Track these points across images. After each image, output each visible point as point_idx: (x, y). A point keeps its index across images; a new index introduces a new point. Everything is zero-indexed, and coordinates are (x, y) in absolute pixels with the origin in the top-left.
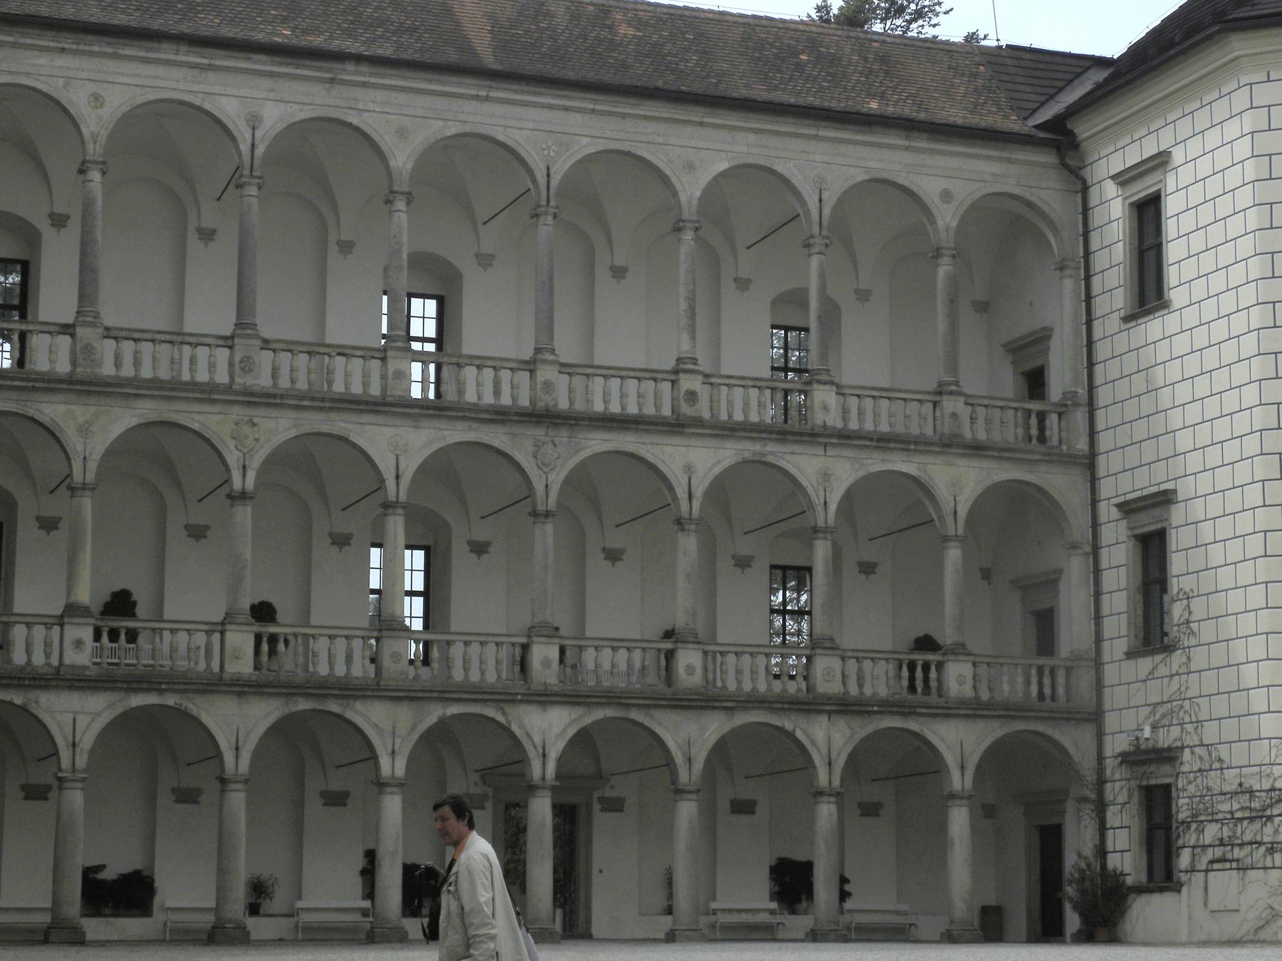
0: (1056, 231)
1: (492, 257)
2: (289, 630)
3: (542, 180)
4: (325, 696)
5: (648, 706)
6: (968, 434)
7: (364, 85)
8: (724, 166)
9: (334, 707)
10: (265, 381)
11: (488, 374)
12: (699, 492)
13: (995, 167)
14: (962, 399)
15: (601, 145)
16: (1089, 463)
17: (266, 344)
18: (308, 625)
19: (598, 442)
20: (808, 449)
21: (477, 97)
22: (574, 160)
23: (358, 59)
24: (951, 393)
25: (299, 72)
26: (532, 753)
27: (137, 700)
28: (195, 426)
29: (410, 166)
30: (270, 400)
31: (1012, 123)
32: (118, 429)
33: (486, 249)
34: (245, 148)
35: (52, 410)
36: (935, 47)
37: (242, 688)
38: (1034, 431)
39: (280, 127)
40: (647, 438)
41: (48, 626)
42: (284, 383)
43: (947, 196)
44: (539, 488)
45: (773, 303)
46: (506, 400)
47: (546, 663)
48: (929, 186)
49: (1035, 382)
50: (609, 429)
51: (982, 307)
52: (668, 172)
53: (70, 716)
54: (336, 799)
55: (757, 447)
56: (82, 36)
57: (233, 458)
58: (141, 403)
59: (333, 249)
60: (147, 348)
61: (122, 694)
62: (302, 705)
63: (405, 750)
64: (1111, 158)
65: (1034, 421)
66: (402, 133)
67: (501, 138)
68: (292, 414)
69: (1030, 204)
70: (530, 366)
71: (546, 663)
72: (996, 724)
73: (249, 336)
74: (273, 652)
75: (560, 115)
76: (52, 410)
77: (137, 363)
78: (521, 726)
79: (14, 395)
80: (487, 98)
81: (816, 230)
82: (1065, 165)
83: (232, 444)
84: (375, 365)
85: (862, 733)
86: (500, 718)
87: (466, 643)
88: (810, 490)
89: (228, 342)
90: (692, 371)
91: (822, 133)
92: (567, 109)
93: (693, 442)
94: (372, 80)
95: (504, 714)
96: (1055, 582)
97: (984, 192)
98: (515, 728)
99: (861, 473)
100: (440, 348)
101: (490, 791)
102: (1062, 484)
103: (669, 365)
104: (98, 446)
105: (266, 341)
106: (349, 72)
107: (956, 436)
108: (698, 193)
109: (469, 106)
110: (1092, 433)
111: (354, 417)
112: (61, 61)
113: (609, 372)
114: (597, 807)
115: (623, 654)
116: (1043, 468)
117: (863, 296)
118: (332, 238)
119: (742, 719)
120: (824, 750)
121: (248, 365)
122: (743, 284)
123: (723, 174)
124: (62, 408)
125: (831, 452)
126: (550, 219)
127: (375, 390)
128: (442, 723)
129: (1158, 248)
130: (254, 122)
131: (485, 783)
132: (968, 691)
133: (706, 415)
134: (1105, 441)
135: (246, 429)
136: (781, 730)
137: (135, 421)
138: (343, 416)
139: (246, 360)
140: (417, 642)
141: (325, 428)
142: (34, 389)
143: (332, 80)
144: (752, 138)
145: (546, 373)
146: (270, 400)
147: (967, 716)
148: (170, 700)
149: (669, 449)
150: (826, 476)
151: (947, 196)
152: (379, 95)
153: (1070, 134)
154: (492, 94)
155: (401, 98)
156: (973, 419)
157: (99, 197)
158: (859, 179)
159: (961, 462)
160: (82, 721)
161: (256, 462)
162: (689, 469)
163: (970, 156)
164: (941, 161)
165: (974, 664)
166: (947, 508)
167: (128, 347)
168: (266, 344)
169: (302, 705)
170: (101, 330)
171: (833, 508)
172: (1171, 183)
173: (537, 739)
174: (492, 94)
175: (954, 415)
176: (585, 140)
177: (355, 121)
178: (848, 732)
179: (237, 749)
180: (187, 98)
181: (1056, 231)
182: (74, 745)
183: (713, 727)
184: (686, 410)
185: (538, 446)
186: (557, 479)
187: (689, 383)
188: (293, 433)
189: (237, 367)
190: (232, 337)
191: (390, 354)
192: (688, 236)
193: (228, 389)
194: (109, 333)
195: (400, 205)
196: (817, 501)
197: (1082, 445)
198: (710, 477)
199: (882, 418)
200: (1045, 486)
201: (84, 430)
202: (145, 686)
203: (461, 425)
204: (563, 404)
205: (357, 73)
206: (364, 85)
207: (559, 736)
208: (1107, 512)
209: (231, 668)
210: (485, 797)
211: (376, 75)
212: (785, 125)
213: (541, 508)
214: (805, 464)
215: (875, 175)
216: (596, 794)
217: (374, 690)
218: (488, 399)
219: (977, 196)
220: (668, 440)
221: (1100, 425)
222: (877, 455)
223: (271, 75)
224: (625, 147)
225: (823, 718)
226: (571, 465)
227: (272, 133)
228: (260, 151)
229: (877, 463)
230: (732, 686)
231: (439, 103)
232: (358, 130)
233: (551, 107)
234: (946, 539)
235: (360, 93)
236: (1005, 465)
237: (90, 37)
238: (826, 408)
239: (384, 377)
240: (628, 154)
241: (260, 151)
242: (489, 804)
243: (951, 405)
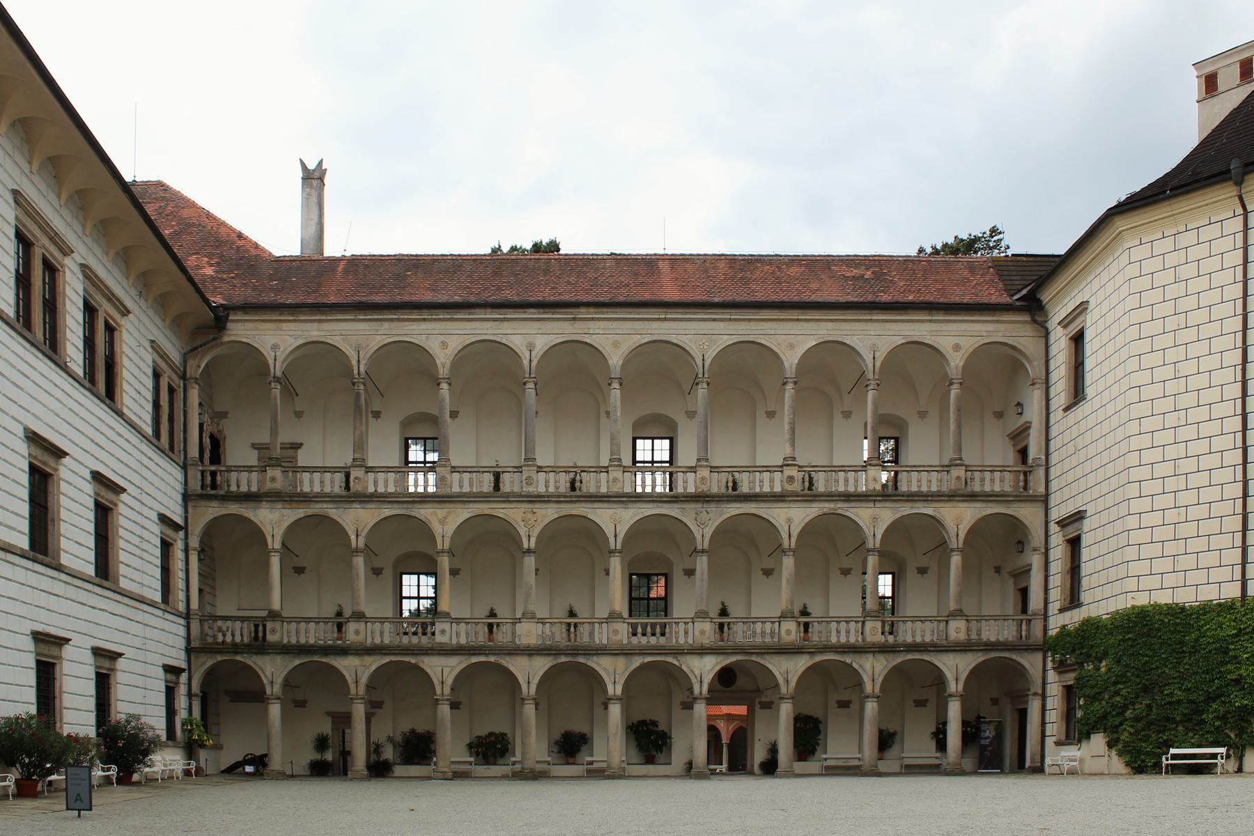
3: (700, 363)
7: (593, 319)
10: (542, 489)
12: (795, 534)
15: (735, 339)
16: (1045, 500)
17: (540, 469)
20: (863, 505)
21: (659, 319)
23: (588, 305)
29: (620, 363)
31: (1005, 299)
34: (526, 362)
35: (423, 512)
40: (762, 505)
42: (551, 489)
44: (699, 538)
50: (740, 501)
55: (832, 505)
57: (523, 532)
58: (472, 505)
64: (1059, 311)
67: (675, 341)
68: (555, 506)
76: (423, 512)
80: (665, 319)
81: (871, 376)
83: (522, 524)
88: (864, 528)
89: (518, 470)
92: (714, 320)
93: (792, 505)
96: (1029, 570)
99: (898, 516)
102: (1028, 514)
104: (450, 528)
106: (583, 313)
109: (655, 325)
110: (1047, 482)
111: (590, 505)
116: (1015, 505)
121: (529, 481)
125: (878, 505)
126: (705, 385)
129: (1082, 363)
134: (1054, 486)
135: (530, 515)
137: (469, 515)
138: (584, 505)
139: (529, 478)
141: (574, 512)
142: (414, 502)
143: (574, 319)
150: (875, 519)
152: (603, 324)
155: (615, 324)
157: (447, 397)
159: (961, 505)
161: (535, 533)
162: (789, 520)
166: (953, 534)
168: (540, 469)
171: (879, 537)
172: (1088, 323)
186: (709, 532)
187: (789, 472)
188: (556, 516)
192: (790, 386)
195: (616, 385)
196: (868, 532)
197: (1042, 489)
198: (803, 524)
201: (443, 522)
203: (650, 505)
205: (588, 313)
206: (593, 319)
208: (1054, 528)
212: (850, 315)
213: (699, 548)
214: (862, 514)
220: (775, 505)
221: (1052, 476)
222: (909, 504)
224: (751, 338)
226: (717, 523)
228: (534, 363)
229: (906, 509)
231: (638, 325)
233: (705, 320)
234: (952, 550)
235: (591, 324)
236: (990, 505)
240: (753, 342)
241: (534, 363)
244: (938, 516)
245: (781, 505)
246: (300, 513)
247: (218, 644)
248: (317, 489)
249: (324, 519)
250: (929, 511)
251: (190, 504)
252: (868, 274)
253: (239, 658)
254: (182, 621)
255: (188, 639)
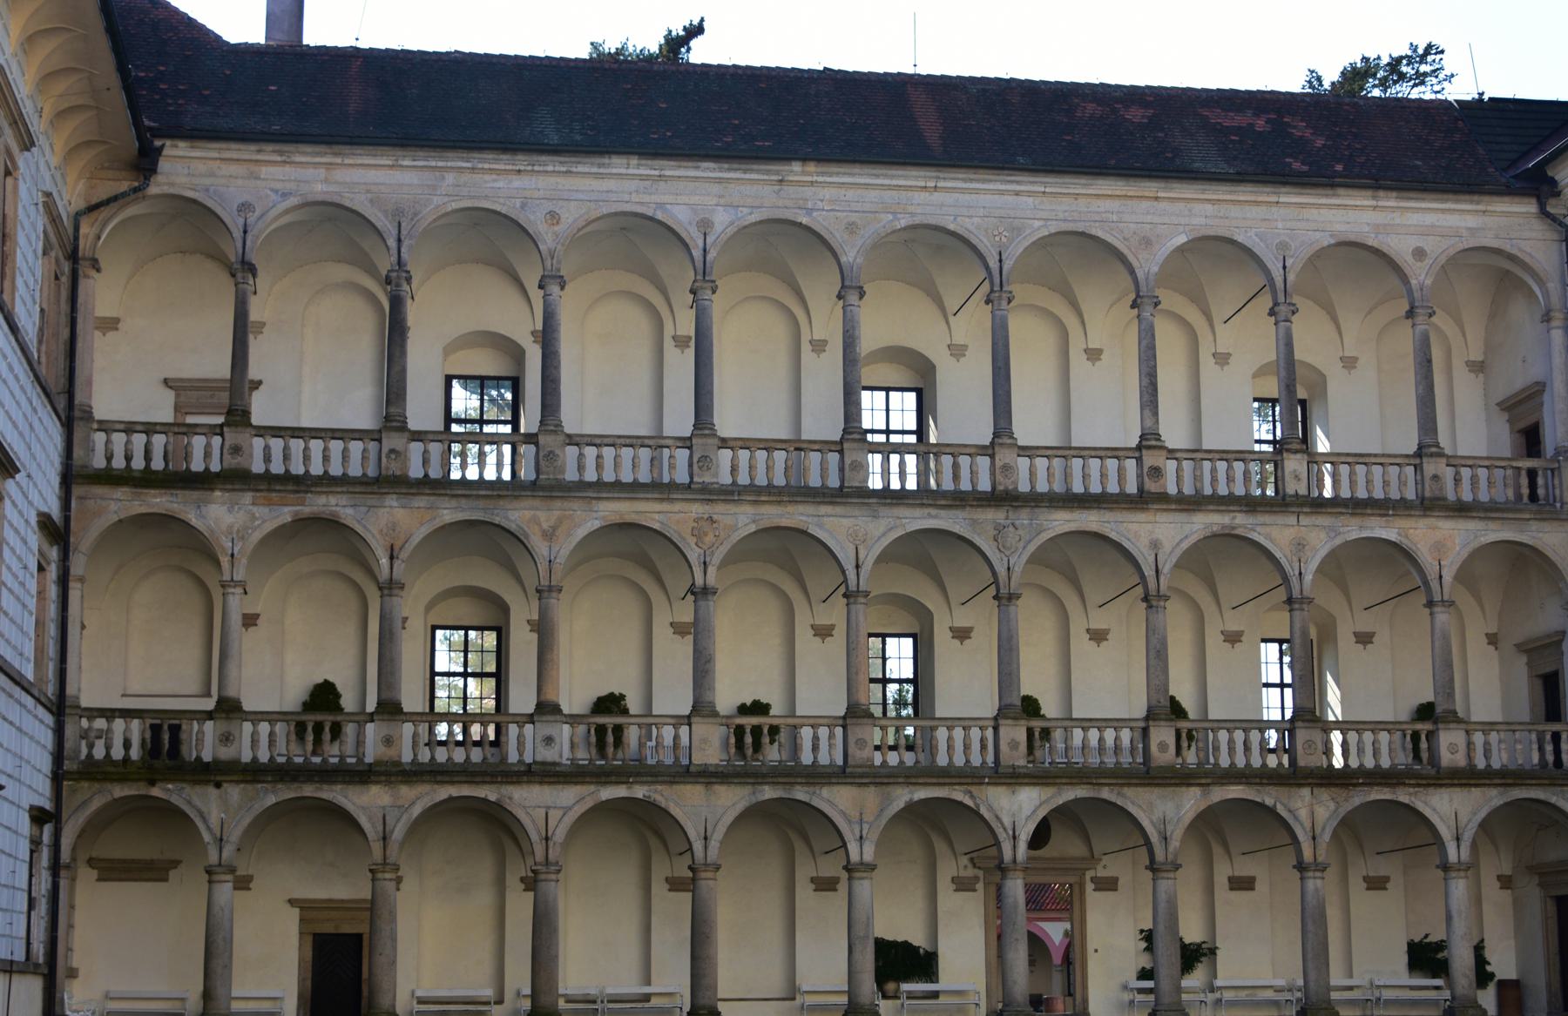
0: (1541, 283)
1: (964, 347)
2: (775, 722)
4: (792, 784)
5: (1122, 785)
6: (1451, 496)
8: (1182, 239)
9: (800, 794)
11: (947, 461)
13: (1471, 221)
14: (1444, 460)
18: (794, 716)
19: (1062, 521)
20: (1280, 519)
22: (1027, 243)
24: (1432, 455)
25: (747, 176)
26: (1002, 836)
27: (609, 793)
28: (656, 526)
30: (731, 493)
32: (581, 533)
33: (959, 339)
35: (517, 515)
36: (1441, 108)
37: (709, 776)
38: (1525, 491)
39: (731, 231)
41: (521, 725)
43: (1419, 253)
45: (1255, 376)
46: (965, 486)
47: (1014, 745)
48: (1400, 246)
49: (1531, 439)
51: (1478, 367)
52: (1125, 251)
53: (543, 811)
54: (825, 885)
56: (535, 158)
57: (694, 555)
59: (806, 347)
60: (608, 452)
61: (592, 788)
62: (768, 793)
63: (873, 836)
65: (1524, 481)
66: (852, 228)
67: (952, 227)
69: (1512, 258)
70: (989, 451)
71: (1014, 745)
72: (1494, 792)
73: (706, 436)
74: (757, 746)
75: (1010, 199)
77: (599, 466)
78: (990, 808)
79: (481, 503)
82: (1544, 213)
84: (833, 458)
85: (1348, 806)
86: (968, 801)
87: (950, 729)
88: (1283, 561)
89: (686, 443)
90: (1154, 447)
91: (1283, 199)
92: (1017, 194)
94: (820, 179)
95: (972, 797)
97: (1461, 247)
98: (983, 811)
99: (1338, 541)
100: (920, 439)
101: (980, 873)
103: (1134, 442)
104: (564, 549)
105: (724, 440)
107: (1438, 499)
108: (1155, 269)
112: (517, 182)
113: (1084, 453)
114: (1090, 887)
115: (1094, 735)
117: (1349, 363)
118: (805, 338)
119: (1220, 794)
120: (1308, 825)
122: (1222, 359)
123: (1181, 250)
124: (528, 514)
125: (1304, 520)
127: (834, 482)
128: (911, 809)
130: (705, 226)
131: (974, 866)
132: (1460, 760)
133: (1172, 489)
136: (1261, 805)
137: (597, 524)
139: (704, 458)
140: (484, 724)
141: (785, 522)
144: (1209, 207)
145: (1004, 456)
146: (731, 493)
147: (1461, 785)
148: (639, 792)
149: (1134, 527)
150: (1300, 545)
151: (1419, 253)
153: (1553, 182)
154: (941, 184)
156: (1457, 480)
158: (1326, 243)
160: (554, 815)
163: (1443, 211)
164: (1414, 219)
165: (1467, 732)
167: (590, 452)
168: (724, 443)
169: (768, 793)
170: (561, 438)
173: (1007, 821)
174: (941, 184)
175: (1435, 477)
176: (1037, 224)
177: (805, 221)
178: (1332, 806)
179: (705, 838)
180: (639, 209)
181: (1541, 283)
182: (547, 839)
183: (1190, 802)
184: (1151, 486)
185: (1000, 529)
186: (1019, 561)
187: (1150, 459)
188: (753, 528)
189: (695, 467)
190: (690, 439)
191: (846, 445)
193: (688, 487)
194: (572, 440)
199: (1375, 482)
200: (1538, 545)
201: (549, 535)
202: (613, 779)
204: (1024, 487)
205: (804, 173)
207: (1028, 818)
209: (698, 759)
210: (976, 878)
211: (823, 174)
215: (1342, 238)
216: (1088, 877)
217: (843, 774)
218: (948, 485)
219: (1452, 252)
222: (1355, 521)
223: (720, 181)
224: (1080, 227)
225: (1306, 791)
226: (1032, 548)
227: (724, 237)
230: (407, 757)
231: (889, 196)
232: (808, 229)
236: (1491, 525)
237: (543, 158)
238: (1297, 478)
239: (842, 470)
240: (1083, 234)
242: (980, 886)
243: (1430, 467)
244: (1405, 543)
245: (1141, 516)
246: (286, 514)
247: (114, 763)
248: (316, 469)
249: (330, 525)
250: (1391, 534)
251: (77, 491)
252: (1261, 124)
253: (156, 792)
254: (49, 719)
255: (58, 756)
